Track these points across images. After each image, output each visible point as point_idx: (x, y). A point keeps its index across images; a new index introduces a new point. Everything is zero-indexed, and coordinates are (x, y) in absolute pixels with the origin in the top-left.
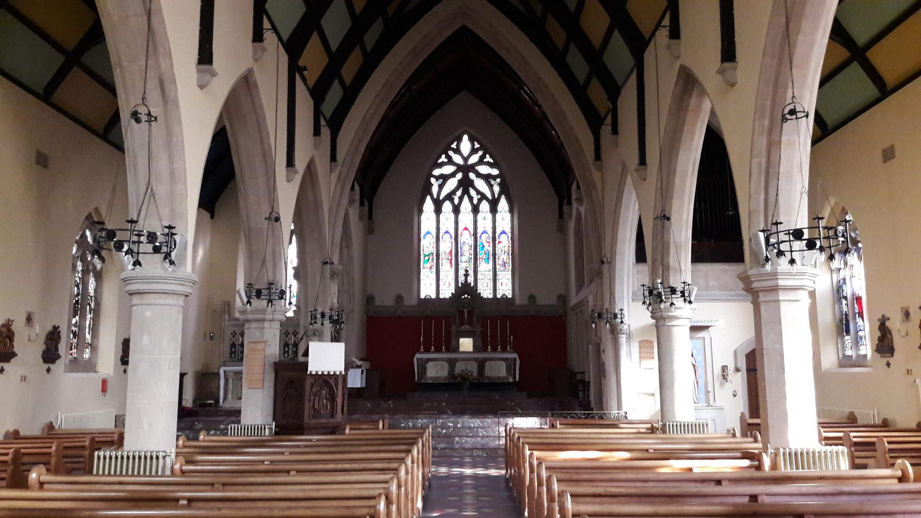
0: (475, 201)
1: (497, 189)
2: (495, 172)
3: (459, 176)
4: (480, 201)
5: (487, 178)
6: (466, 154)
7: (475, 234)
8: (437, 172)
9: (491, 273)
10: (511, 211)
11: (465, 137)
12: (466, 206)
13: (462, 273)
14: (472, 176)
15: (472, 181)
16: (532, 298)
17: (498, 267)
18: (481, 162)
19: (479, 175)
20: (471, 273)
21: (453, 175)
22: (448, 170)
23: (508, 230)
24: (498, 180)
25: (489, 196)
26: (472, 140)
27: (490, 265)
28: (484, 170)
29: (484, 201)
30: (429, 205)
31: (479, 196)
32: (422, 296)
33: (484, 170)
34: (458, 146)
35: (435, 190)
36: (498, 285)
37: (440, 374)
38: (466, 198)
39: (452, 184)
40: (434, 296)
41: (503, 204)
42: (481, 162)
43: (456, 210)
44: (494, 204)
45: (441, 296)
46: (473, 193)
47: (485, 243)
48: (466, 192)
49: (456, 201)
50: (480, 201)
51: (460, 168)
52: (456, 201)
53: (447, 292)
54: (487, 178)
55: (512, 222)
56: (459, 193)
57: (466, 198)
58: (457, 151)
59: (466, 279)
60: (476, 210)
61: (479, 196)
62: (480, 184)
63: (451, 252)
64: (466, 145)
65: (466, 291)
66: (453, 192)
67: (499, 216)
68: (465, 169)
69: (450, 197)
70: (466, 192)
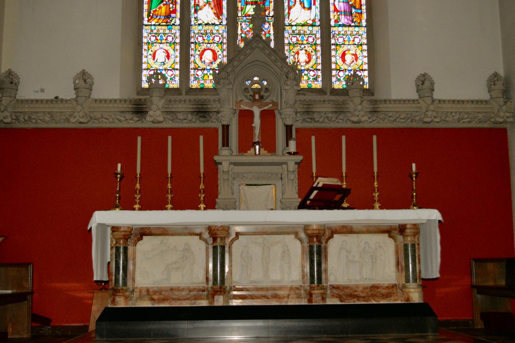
9: (316, 30)
13: (244, 28)
16: (424, 83)
17: (333, 16)
20: (269, 28)
36: (336, 58)
45: (194, 84)
59: (258, 29)
65: (256, 55)
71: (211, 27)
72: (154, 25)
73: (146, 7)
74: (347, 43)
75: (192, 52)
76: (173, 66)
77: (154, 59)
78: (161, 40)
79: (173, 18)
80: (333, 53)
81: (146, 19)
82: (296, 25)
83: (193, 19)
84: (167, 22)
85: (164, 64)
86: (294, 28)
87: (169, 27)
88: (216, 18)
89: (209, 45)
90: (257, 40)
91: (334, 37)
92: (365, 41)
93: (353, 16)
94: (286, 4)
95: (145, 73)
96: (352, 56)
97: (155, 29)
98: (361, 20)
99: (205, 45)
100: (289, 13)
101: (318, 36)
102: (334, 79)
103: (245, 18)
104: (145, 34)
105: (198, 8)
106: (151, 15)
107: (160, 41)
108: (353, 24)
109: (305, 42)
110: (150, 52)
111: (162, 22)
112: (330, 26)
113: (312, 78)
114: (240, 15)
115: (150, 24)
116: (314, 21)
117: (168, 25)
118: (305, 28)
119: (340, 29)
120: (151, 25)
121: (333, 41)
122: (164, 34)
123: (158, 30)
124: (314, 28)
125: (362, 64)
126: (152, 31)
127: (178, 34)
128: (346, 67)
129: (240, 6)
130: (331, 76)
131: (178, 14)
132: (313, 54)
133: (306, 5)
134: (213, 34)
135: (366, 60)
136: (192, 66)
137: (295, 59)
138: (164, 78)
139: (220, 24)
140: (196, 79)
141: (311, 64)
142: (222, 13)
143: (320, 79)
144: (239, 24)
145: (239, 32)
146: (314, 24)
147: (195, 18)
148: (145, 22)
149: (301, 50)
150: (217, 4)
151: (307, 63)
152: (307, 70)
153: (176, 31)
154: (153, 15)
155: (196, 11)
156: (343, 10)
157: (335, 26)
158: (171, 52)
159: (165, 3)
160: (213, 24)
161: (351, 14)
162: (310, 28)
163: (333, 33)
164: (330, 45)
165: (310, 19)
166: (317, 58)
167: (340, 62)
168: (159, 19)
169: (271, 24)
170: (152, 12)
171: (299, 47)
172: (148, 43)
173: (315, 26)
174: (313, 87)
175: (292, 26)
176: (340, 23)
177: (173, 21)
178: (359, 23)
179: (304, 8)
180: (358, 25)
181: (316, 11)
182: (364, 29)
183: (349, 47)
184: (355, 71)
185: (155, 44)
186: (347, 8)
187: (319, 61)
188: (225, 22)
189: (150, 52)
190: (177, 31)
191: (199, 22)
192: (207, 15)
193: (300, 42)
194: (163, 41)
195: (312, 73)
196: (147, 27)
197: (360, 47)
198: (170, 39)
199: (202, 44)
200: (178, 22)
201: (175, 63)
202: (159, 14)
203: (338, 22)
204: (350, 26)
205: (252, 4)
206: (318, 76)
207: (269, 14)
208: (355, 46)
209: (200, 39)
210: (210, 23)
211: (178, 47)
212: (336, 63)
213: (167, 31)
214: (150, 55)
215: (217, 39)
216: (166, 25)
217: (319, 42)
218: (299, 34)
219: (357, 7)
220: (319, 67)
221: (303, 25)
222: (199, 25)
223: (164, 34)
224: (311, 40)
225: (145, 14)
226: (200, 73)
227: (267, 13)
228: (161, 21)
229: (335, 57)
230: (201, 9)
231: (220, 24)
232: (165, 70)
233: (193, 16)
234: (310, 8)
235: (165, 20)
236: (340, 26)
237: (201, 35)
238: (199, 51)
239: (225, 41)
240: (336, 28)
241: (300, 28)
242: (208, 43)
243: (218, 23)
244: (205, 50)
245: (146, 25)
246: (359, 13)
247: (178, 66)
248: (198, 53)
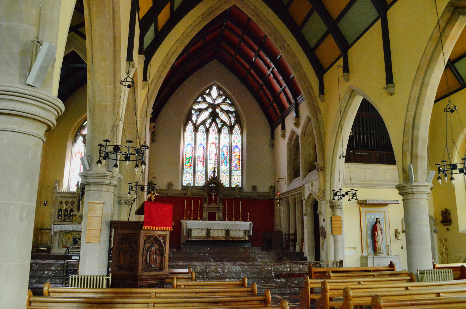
0: (220, 126)
1: (233, 120)
2: (232, 109)
3: (210, 110)
4: (222, 126)
7: (218, 147)
8: (196, 107)
9: (228, 171)
10: (242, 133)
11: (214, 88)
12: (213, 129)
14: (218, 111)
15: (218, 114)
16: (254, 187)
17: (232, 168)
19: (222, 110)
21: (206, 109)
22: (204, 106)
23: (239, 145)
24: (234, 114)
25: (228, 124)
26: (219, 88)
27: (228, 167)
28: (225, 107)
29: (225, 127)
30: (190, 127)
31: (222, 124)
32: (184, 184)
33: (225, 107)
34: (210, 92)
35: (194, 118)
36: (233, 179)
37: (200, 235)
38: (214, 125)
39: (205, 115)
40: (192, 185)
41: (237, 129)
43: (207, 131)
44: (231, 128)
45: (196, 185)
46: (218, 121)
48: (214, 120)
49: (207, 125)
50: (222, 126)
51: (211, 105)
52: (207, 125)
53: (200, 182)
54: (228, 112)
55: (242, 140)
57: (214, 125)
58: (209, 94)
60: (220, 131)
61: (222, 124)
62: (223, 116)
64: (214, 92)
68: (213, 106)
69: (203, 123)
70: (214, 120)
96: (237, 181)
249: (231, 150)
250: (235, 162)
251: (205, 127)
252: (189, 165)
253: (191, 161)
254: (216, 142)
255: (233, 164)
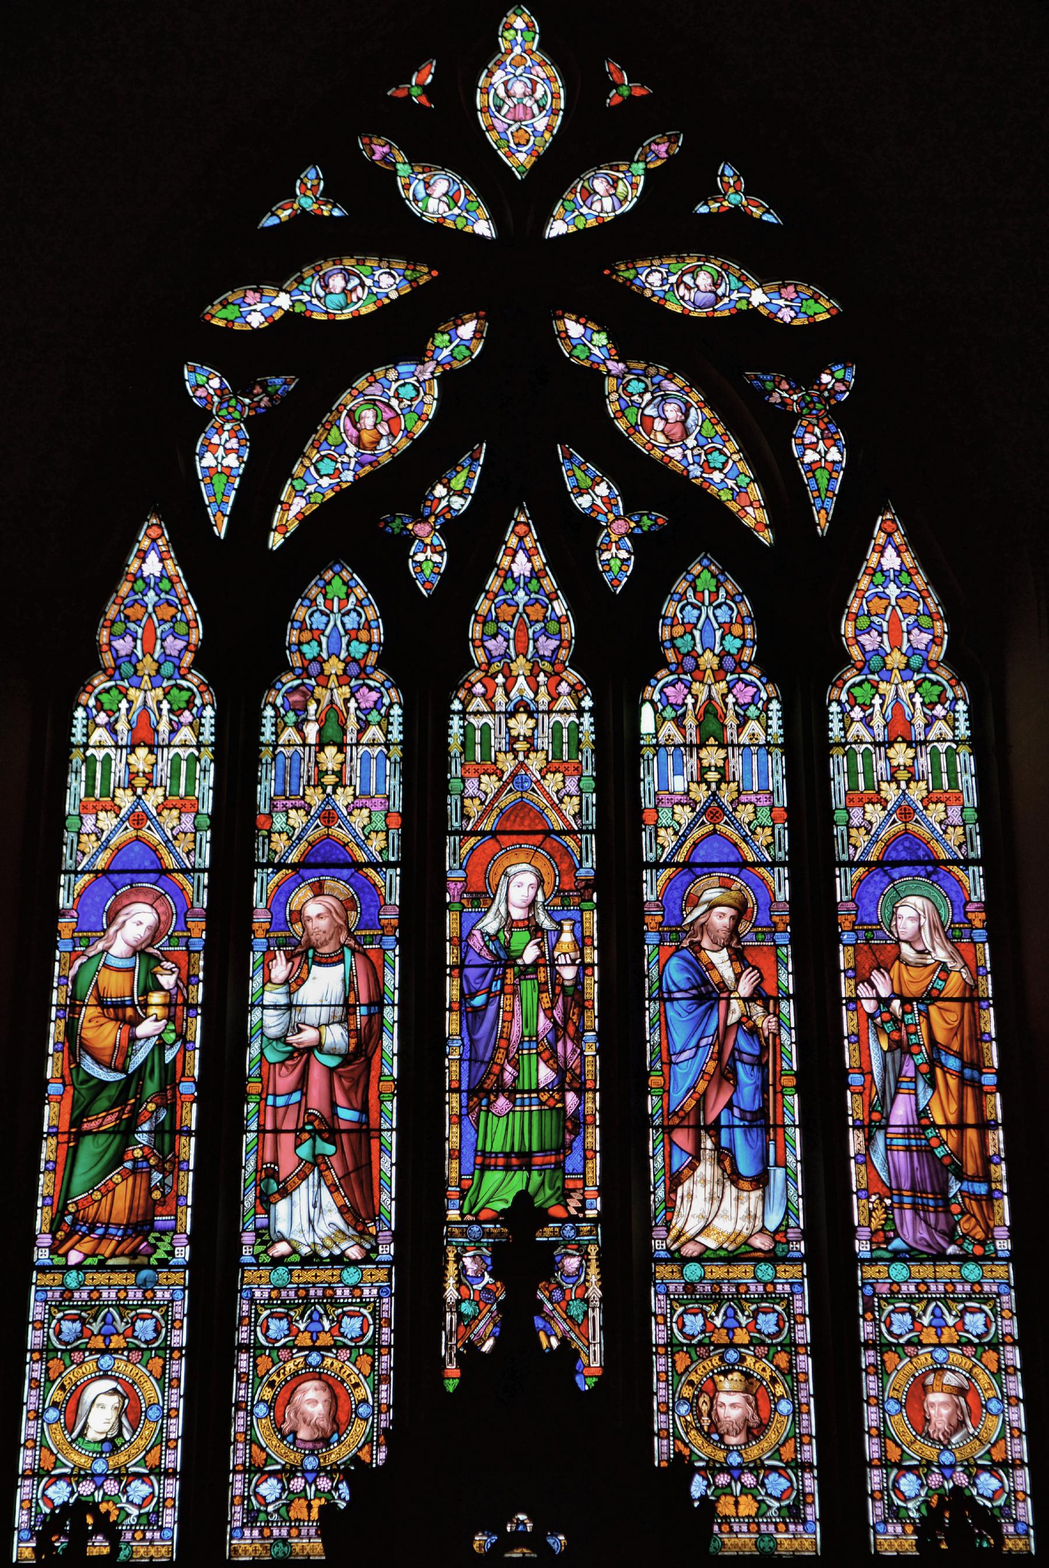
0: (616, 560)
1: (821, 455)
4: (658, 565)
5: (719, 358)
6: (521, 160)
11: (519, 30)
13: (468, 1279)
14: (582, 338)
18: (663, 224)
19: (652, 336)
20: (581, 1272)
21: (396, 334)
22: (356, 289)
23: (950, 825)
28: (690, 286)
33: (690, 286)
35: (221, 457)
38: (521, 558)
39: (387, 411)
42: (663, 224)
43: (427, 656)
46: (594, 494)
47: (721, 961)
48: (522, 485)
52: (428, 560)
54: (719, 358)
56: (453, 494)
57: (521, 558)
58: (454, 139)
60: (618, 651)
62: (673, 423)
63: (362, 1052)
64: (521, 96)
66: (397, 485)
67: (852, 720)
68: (517, 277)
69: (360, 528)
71: (325, 1275)
72: (79, 1267)
73: (45, 1184)
74: (929, 1337)
75: (239, 1392)
76: (152, 1459)
77: (70, 1428)
78: (107, 1337)
79: (164, 1232)
80: (870, 1385)
81: (45, 1240)
82: (699, 1259)
83: (248, 1238)
84: (134, 1254)
85: (115, 1449)
86: (693, 1271)
87: (144, 1273)
88: (351, 1232)
89: (314, 1358)
90: (522, 1363)
91: (869, 1308)
92: (1011, 1327)
93: (955, 1209)
94: (657, 1164)
95: (24, 1491)
97: (82, 1284)
98: (989, 1230)
99: (299, 1357)
100: (670, 1206)
101: (802, 1305)
102: (875, 1511)
103: (476, 1228)
104: (36, 1310)
105: (274, 1187)
106: (68, 1219)
107: (99, 1343)
108: (952, 1250)
109: (741, 1337)
110: (55, 1394)
111: (113, 1255)
112: (854, 1261)
113: (776, 1504)
114: (453, 1214)
115: (58, 1261)
116: (779, 1234)
117: (136, 1269)
118: (741, 1272)
119: (899, 1271)
120: (67, 1268)
121: (866, 1330)
122: (122, 1307)
123: (96, 1289)
124: (781, 1268)
125: (1002, 1437)
126: (67, 1293)
127: (181, 1308)
128: (930, 1452)
129: (454, 1175)
130: (860, 1495)
131: (187, 1221)
132: (779, 1390)
133: (746, 1166)
134: (335, 1304)
135: (1018, 1416)
136: (238, 1457)
137: (699, 1415)
138: (111, 1530)
139: (367, 1260)
140: (252, 1517)
141: (772, 1437)
142: (375, 1215)
143: (813, 1512)
144: (451, 1256)
145: (451, 1293)
146: (780, 1250)
147: (258, 1233)
148: (42, 1256)
149: (725, 1373)
150: (357, 1169)
151: (753, 1432)
152: (757, 1467)
153: (174, 1292)
154: (75, 1221)
155: (265, 1201)
156: (906, 1184)
157: (873, 1261)
158: (150, 1390)
159: (128, 1165)
160: (340, 1261)
161: (944, 1201)
162: (765, 1271)
163: (868, 1291)
164: (856, 1346)
165: (763, 1230)
166: (797, 1412)
167: (900, 1426)
168: (102, 1237)
169: (593, 1256)
170: (72, 1208)
171: (716, 1361)
172: (46, 1351)
173: (785, 1260)
174: (782, 1551)
175: (686, 1260)
176: (897, 1244)
177: (164, 1247)
178: (982, 1243)
179: (735, 1177)
180: (979, 1251)
181: (786, 1185)
182: (1006, 1272)
183: (940, 1355)
184: (973, 1469)
185: (76, 1356)
186: (923, 1174)
187: (810, 1423)
188: (387, 1251)
189: (55, 1394)
190: (179, 1295)
191: (282, 1248)
192: (307, 1217)
193: (722, 1337)
194: (116, 1342)
195: (777, 1484)
196: (47, 1279)
197: (991, 1355)
198: (145, 1329)
199: (284, 1354)
200: (183, 1254)
201: (163, 1442)
202: (104, 1216)
203: (888, 1241)
204: (940, 1257)
205: (507, 1168)
206: (803, 1497)
207: (582, 1209)
208: (969, 1351)
209: (277, 1327)
210: (325, 1254)
211: (179, 1368)
212: (883, 1435)
213: (135, 1295)
214: (55, 1405)
215: (352, 1326)
216: (129, 1268)
217: (804, 1333)
218: (717, 1298)
219: (971, 1168)
220: (810, 1453)
221: (732, 1259)
222: (278, 1262)
223: (122, 1307)
224: (767, 1323)
225: (42, 1220)
226: (270, 1489)
227: (573, 1203)
228: (107, 1248)
229: (880, 1404)
230: (285, 1193)
231: (367, 1260)
232: (118, 1478)
233: (249, 1221)
234: (761, 1181)
235: (127, 1246)
236: (897, 1256)
237: (283, 1308)
238: (271, 1385)
239: (387, 1336)
240: (881, 1267)
241: (718, 1271)
242: (312, 1349)
243: (354, 1253)
244: (298, 1378)
245: (43, 1269)
246: (977, 1198)
247: (173, 1459)
248: (268, 1394)
249: (814, 925)
250: (901, 1112)
251: (388, 578)
252: (121, 1198)
253: (167, 1133)
254: (568, 798)
255: (875, 1161)
